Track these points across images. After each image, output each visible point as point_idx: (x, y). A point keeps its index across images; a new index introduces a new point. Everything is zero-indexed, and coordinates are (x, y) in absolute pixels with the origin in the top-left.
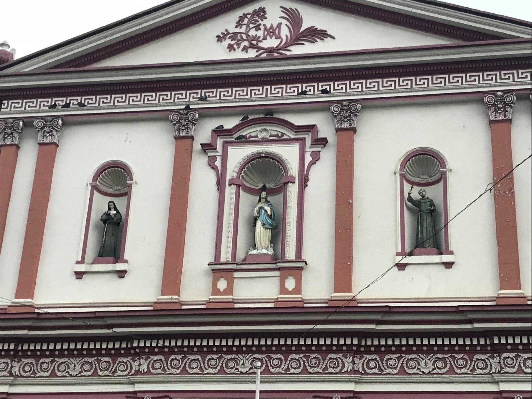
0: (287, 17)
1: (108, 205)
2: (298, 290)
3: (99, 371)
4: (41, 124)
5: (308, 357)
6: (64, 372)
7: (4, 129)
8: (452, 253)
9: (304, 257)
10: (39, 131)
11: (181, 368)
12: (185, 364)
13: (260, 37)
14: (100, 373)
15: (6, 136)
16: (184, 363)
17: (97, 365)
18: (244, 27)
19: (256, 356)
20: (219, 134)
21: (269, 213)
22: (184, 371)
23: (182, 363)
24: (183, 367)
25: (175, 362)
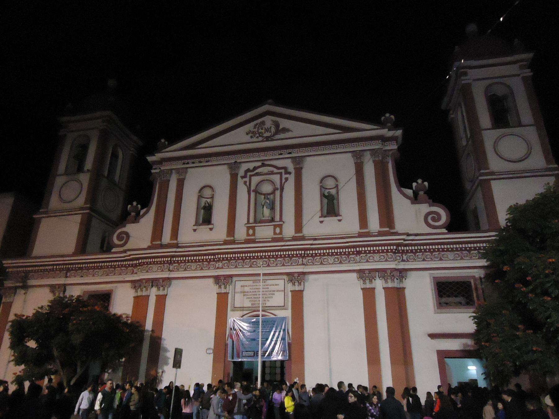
2: (281, 233)
5: (284, 259)
8: (341, 216)
14: (203, 269)
19: (264, 260)
22: (236, 267)
25: (232, 263)
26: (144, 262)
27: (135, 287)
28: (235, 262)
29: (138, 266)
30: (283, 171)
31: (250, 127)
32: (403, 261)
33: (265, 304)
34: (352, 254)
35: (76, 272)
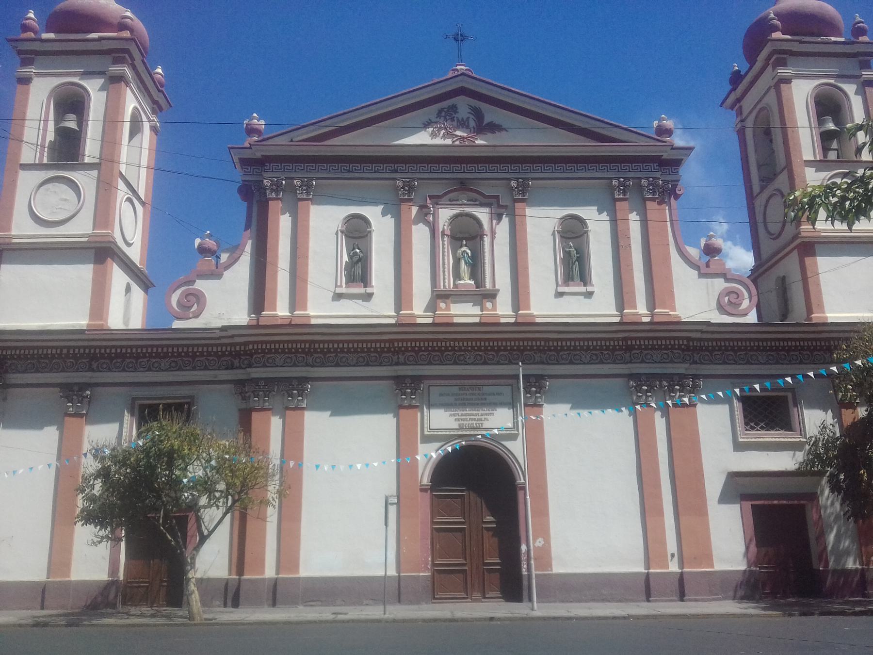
2: (494, 308)
4: (299, 183)
8: (593, 286)
9: (497, 287)
14: (371, 363)
18: (442, 118)
19: (477, 353)
21: (470, 255)
22: (430, 363)
25: (423, 357)
26: (258, 349)
27: (240, 393)
30: (493, 201)
32: (695, 363)
33: (482, 424)
34: (619, 350)
35: (111, 362)
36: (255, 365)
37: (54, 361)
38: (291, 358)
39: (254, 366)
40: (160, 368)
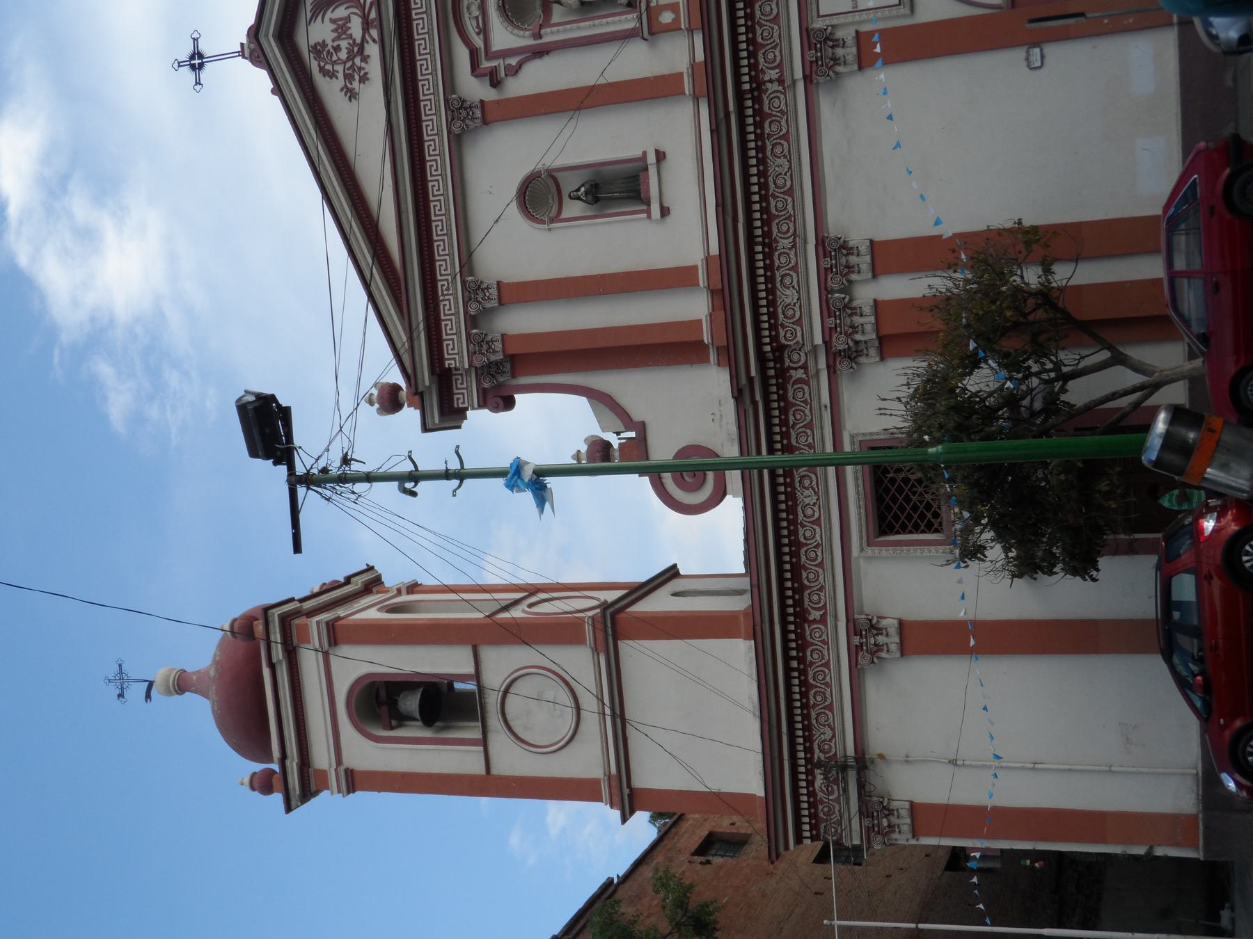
0: (322, 13)
1: (574, 199)
3: (781, 133)
6: (786, 178)
7: (483, 354)
10: (482, 307)
11: (772, 25)
12: (767, 21)
13: (349, 43)
14: (784, 131)
15: (491, 350)
16: (765, 23)
17: (775, 137)
20: (477, 66)
22: (776, 20)
23: (766, 26)
24: (771, 23)
25: (765, 34)
27: (852, 359)
28: (761, 25)
29: (782, 362)
31: (330, 91)
36: (799, 338)
37: (811, 681)
38: (783, 276)
39: (801, 342)
40: (814, 504)
